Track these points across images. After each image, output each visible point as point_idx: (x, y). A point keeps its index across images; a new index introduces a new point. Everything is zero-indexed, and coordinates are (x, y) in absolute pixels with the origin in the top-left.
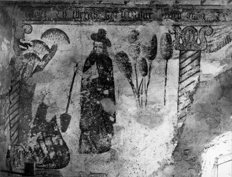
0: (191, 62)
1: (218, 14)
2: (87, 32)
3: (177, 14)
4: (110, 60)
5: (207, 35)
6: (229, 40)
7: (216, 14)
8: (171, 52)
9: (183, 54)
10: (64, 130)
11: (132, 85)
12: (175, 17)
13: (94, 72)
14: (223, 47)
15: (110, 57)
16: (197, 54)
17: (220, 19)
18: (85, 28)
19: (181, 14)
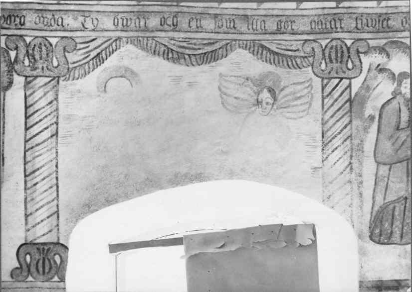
0: (45, 94)
1: (84, 18)
3: (17, 16)
5: (68, 52)
6: (102, 60)
7: (81, 19)
8: (11, 79)
9: (30, 82)
12: (14, 21)
14: (93, 70)
16: (52, 82)
17: (86, 26)
19: (24, 17)
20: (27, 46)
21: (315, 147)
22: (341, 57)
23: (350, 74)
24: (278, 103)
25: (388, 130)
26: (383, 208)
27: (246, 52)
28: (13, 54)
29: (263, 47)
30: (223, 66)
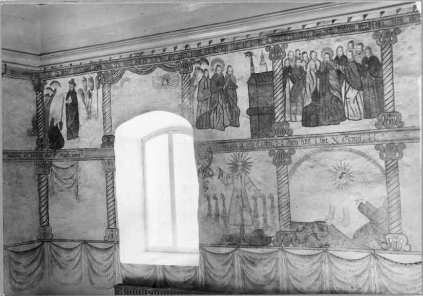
4: (76, 93)
10: (61, 129)
11: (85, 104)
13: (70, 100)
15: (76, 91)
18: (66, 79)
20: (103, 74)
22: (186, 67)
25: (201, 89)
26: (200, 116)
28: (100, 78)
30: (153, 74)
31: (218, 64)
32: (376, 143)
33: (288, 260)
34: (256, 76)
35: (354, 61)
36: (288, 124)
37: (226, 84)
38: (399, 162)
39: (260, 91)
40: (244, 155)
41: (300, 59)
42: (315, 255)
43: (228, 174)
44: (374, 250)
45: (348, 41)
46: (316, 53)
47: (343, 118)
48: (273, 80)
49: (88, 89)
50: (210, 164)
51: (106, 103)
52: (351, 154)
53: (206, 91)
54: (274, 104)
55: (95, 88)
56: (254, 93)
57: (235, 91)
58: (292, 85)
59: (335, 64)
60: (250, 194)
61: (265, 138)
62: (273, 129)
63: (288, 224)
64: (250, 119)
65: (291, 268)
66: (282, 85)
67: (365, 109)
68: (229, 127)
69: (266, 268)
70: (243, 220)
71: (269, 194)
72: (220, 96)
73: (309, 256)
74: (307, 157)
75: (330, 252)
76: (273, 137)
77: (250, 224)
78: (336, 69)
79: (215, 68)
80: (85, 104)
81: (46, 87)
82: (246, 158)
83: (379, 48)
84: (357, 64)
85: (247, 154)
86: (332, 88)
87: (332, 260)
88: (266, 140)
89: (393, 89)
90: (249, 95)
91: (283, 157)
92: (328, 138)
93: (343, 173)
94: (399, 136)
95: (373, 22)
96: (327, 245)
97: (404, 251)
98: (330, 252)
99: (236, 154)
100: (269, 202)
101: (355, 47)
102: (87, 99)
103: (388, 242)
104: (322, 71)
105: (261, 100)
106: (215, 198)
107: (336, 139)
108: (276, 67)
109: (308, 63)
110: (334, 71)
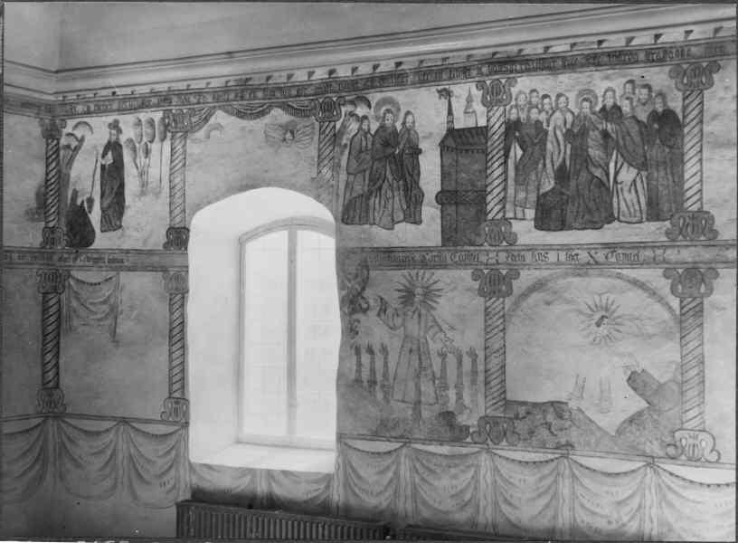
2: (104, 122)
4: (120, 146)
10: (90, 212)
11: (137, 167)
15: (122, 143)
18: (104, 118)
20: (174, 115)
21: (314, 165)
22: (329, 109)
23: (334, 119)
24: (296, 139)
26: (350, 201)
27: (279, 110)
28: (167, 121)
29: (289, 106)
30: (267, 119)
31: (389, 107)
32: (667, 266)
33: (496, 470)
34: (456, 133)
35: (634, 117)
36: (510, 223)
37: (401, 147)
38: (706, 301)
39: (463, 160)
40: (427, 275)
41: (537, 108)
42: (547, 462)
43: (396, 309)
44: (653, 457)
45: (624, 80)
46: (567, 99)
47: (610, 219)
48: (487, 143)
49: (145, 139)
50: (363, 289)
51: (176, 168)
52: (618, 282)
53: (363, 155)
54: (487, 186)
55: (157, 139)
56: (451, 164)
57: (418, 158)
58: (520, 152)
59: (599, 120)
60: (434, 346)
61: (468, 248)
62: (482, 232)
63: (500, 403)
64: (442, 212)
65: (502, 484)
66: (502, 152)
67: (650, 203)
68: (404, 223)
69: (454, 482)
70: (419, 392)
71: (468, 350)
72: (388, 167)
73: (535, 463)
74: (539, 286)
75: (574, 457)
76: (482, 245)
77: (432, 401)
78: (600, 127)
79: (382, 115)
80: (137, 167)
81: (65, 131)
82: (431, 281)
83: (680, 94)
84: (638, 122)
85: (433, 274)
86: (593, 163)
87: (577, 472)
88: (469, 251)
89: (701, 171)
90: (442, 166)
91: (497, 283)
92: (579, 252)
93: (603, 317)
94: (707, 255)
95: (671, 47)
96: (570, 445)
97: (707, 461)
98: (574, 457)
99: (413, 272)
100: (467, 361)
101: (637, 91)
102: (141, 160)
103: (678, 444)
104: (575, 131)
105: (463, 178)
106: (370, 351)
107: (594, 255)
108: (493, 120)
109: (551, 116)
110: (597, 133)
